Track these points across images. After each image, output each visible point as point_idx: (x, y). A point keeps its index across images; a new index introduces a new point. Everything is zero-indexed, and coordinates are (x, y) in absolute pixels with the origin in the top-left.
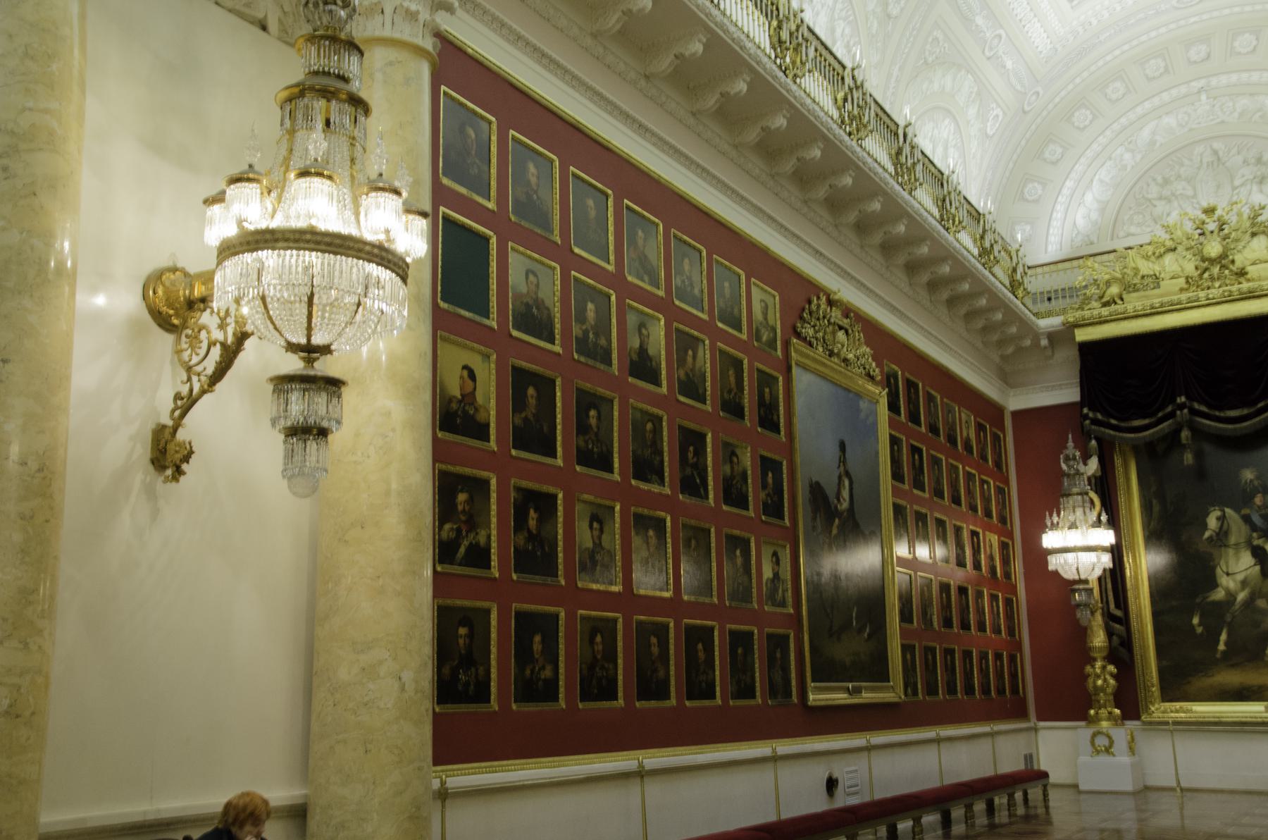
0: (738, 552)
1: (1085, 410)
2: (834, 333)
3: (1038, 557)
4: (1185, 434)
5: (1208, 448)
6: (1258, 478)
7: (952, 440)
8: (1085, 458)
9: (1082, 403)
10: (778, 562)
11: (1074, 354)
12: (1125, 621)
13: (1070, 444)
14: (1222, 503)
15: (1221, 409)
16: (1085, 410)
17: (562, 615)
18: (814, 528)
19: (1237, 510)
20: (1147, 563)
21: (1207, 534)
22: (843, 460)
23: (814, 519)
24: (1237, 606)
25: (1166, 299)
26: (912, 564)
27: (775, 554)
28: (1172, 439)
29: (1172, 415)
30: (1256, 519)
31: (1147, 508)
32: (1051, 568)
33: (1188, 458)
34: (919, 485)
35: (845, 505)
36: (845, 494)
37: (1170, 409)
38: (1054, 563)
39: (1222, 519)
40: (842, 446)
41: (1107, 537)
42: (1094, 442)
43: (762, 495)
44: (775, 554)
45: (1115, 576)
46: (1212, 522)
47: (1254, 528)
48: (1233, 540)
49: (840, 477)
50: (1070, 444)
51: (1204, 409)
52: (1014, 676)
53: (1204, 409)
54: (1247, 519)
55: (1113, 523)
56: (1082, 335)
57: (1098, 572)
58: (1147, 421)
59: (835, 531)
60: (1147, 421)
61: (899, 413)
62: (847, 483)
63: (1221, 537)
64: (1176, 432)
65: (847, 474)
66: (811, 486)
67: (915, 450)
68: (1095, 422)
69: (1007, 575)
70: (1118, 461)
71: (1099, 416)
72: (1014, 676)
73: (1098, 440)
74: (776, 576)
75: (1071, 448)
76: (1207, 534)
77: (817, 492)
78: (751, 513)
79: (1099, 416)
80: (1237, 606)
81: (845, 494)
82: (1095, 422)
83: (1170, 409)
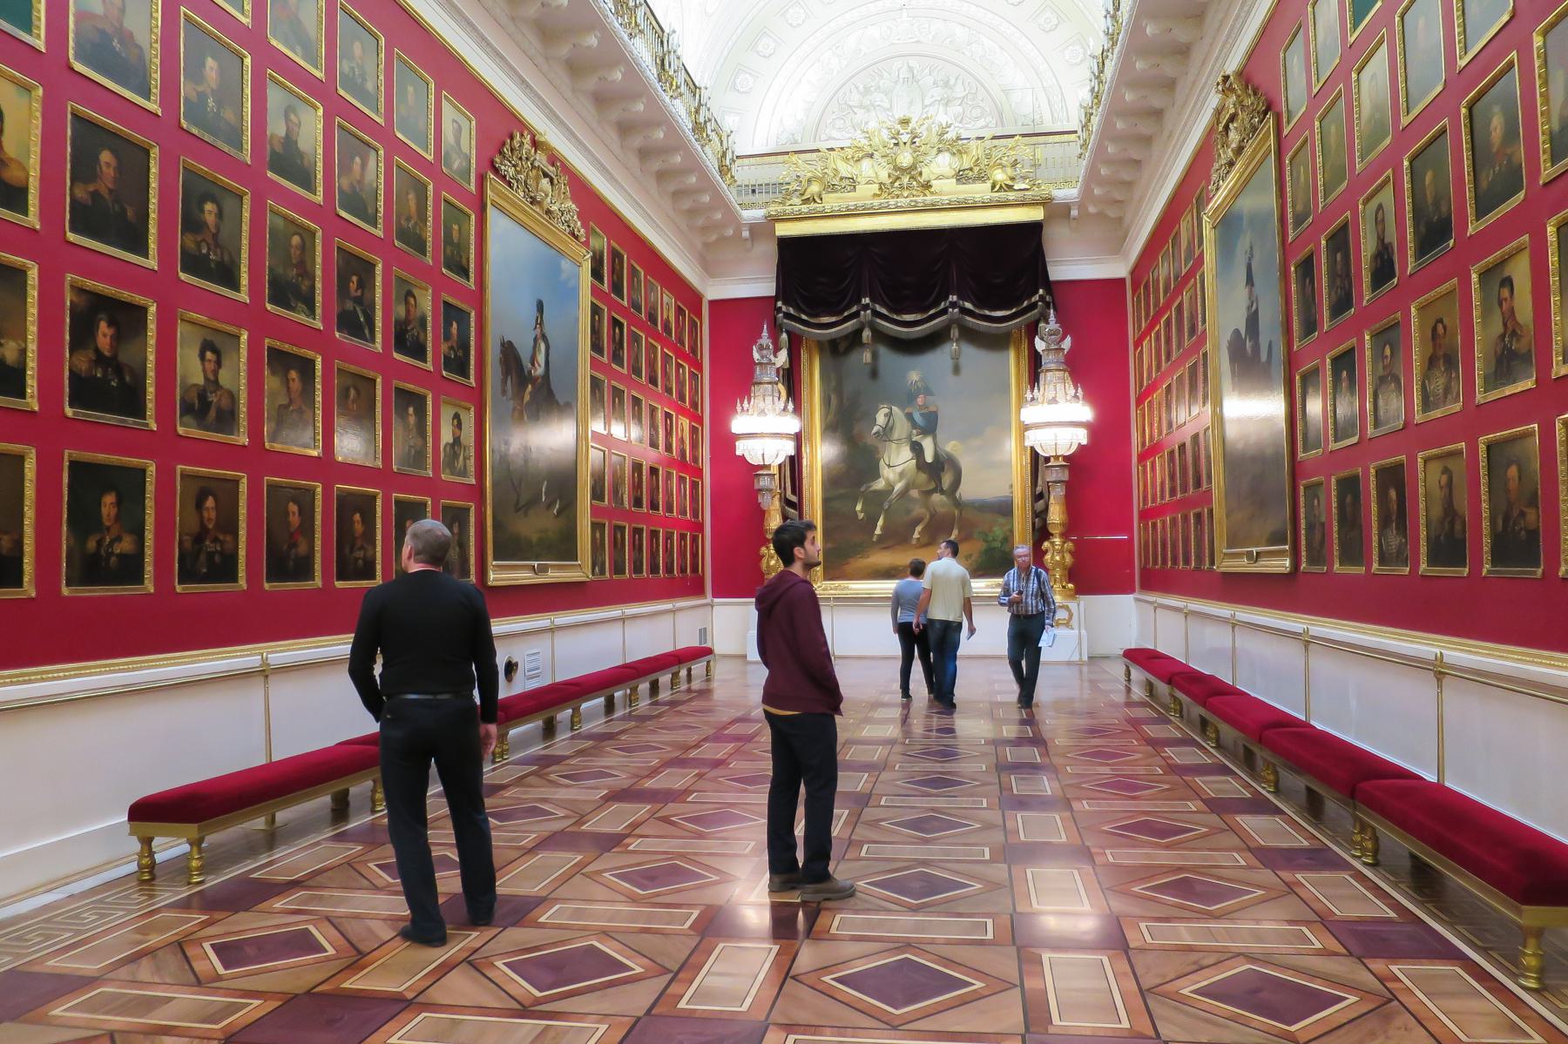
0: (411, 410)
1: (779, 304)
2: (537, 179)
3: (724, 442)
4: (867, 334)
5: (883, 351)
6: (922, 380)
7: (652, 318)
8: (777, 350)
9: (776, 298)
10: (459, 426)
11: (772, 250)
12: (798, 506)
13: (765, 334)
14: (891, 401)
15: (899, 312)
16: (779, 304)
17: (152, 469)
18: (504, 392)
19: (902, 408)
20: (822, 454)
21: (876, 429)
22: (540, 322)
23: (504, 382)
24: (894, 495)
25: (860, 203)
26: (605, 440)
27: (457, 416)
28: (854, 339)
29: (856, 315)
30: (917, 417)
31: (826, 401)
32: (738, 453)
33: (867, 356)
34: (616, 358)
35: (540, 371)
36: (541, 358)
37: (855, 309)
38: (741, 448)
39: (889, 415)
40: (540, 307)
41: (792, 424)
42: (784, 336)
43: (444, 347)
44: (457, 416)
45: (795, 462)
46: (881, 418)
47: (914, 425)
48: (896, 436)
49: (535, 340)
50: (765, 334)
51: (884, 311)
52: (694, 555)
53: (884, 311)
54: (909, 417)
55: (798, 410)
56: (784, 230)
57: (780, 460)
58: (833, 319)
59: (527, 398)
60: (833, 319)
61: (602, 281)
62: (543, 346)
63: (888, 430)
64: (857, 333)
65: (544, 337)
66: (503, 345)
67: (616, 323)
68: (788, 316)
69: (695, 459)
70: (804, 356)
71: (791, 311)
72: (694, 555)
73: (788, 333)
74: (457, 441)
75: (765, 339)
76: (876, 429)
77: (509, 352)
78: (429, 366)
79: (791, 311)
80: (894, 495)
81: (541, 358)
82: (788, 316)
83: (855, 309)
